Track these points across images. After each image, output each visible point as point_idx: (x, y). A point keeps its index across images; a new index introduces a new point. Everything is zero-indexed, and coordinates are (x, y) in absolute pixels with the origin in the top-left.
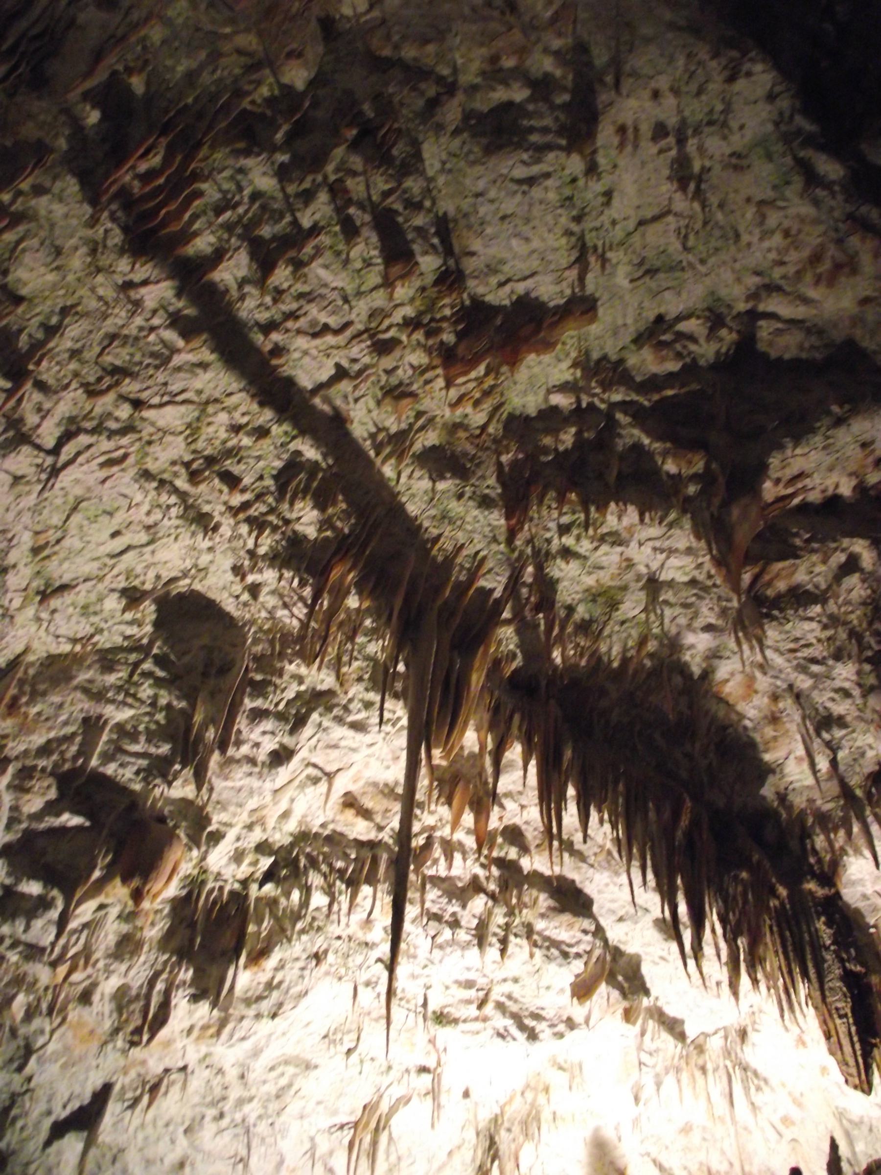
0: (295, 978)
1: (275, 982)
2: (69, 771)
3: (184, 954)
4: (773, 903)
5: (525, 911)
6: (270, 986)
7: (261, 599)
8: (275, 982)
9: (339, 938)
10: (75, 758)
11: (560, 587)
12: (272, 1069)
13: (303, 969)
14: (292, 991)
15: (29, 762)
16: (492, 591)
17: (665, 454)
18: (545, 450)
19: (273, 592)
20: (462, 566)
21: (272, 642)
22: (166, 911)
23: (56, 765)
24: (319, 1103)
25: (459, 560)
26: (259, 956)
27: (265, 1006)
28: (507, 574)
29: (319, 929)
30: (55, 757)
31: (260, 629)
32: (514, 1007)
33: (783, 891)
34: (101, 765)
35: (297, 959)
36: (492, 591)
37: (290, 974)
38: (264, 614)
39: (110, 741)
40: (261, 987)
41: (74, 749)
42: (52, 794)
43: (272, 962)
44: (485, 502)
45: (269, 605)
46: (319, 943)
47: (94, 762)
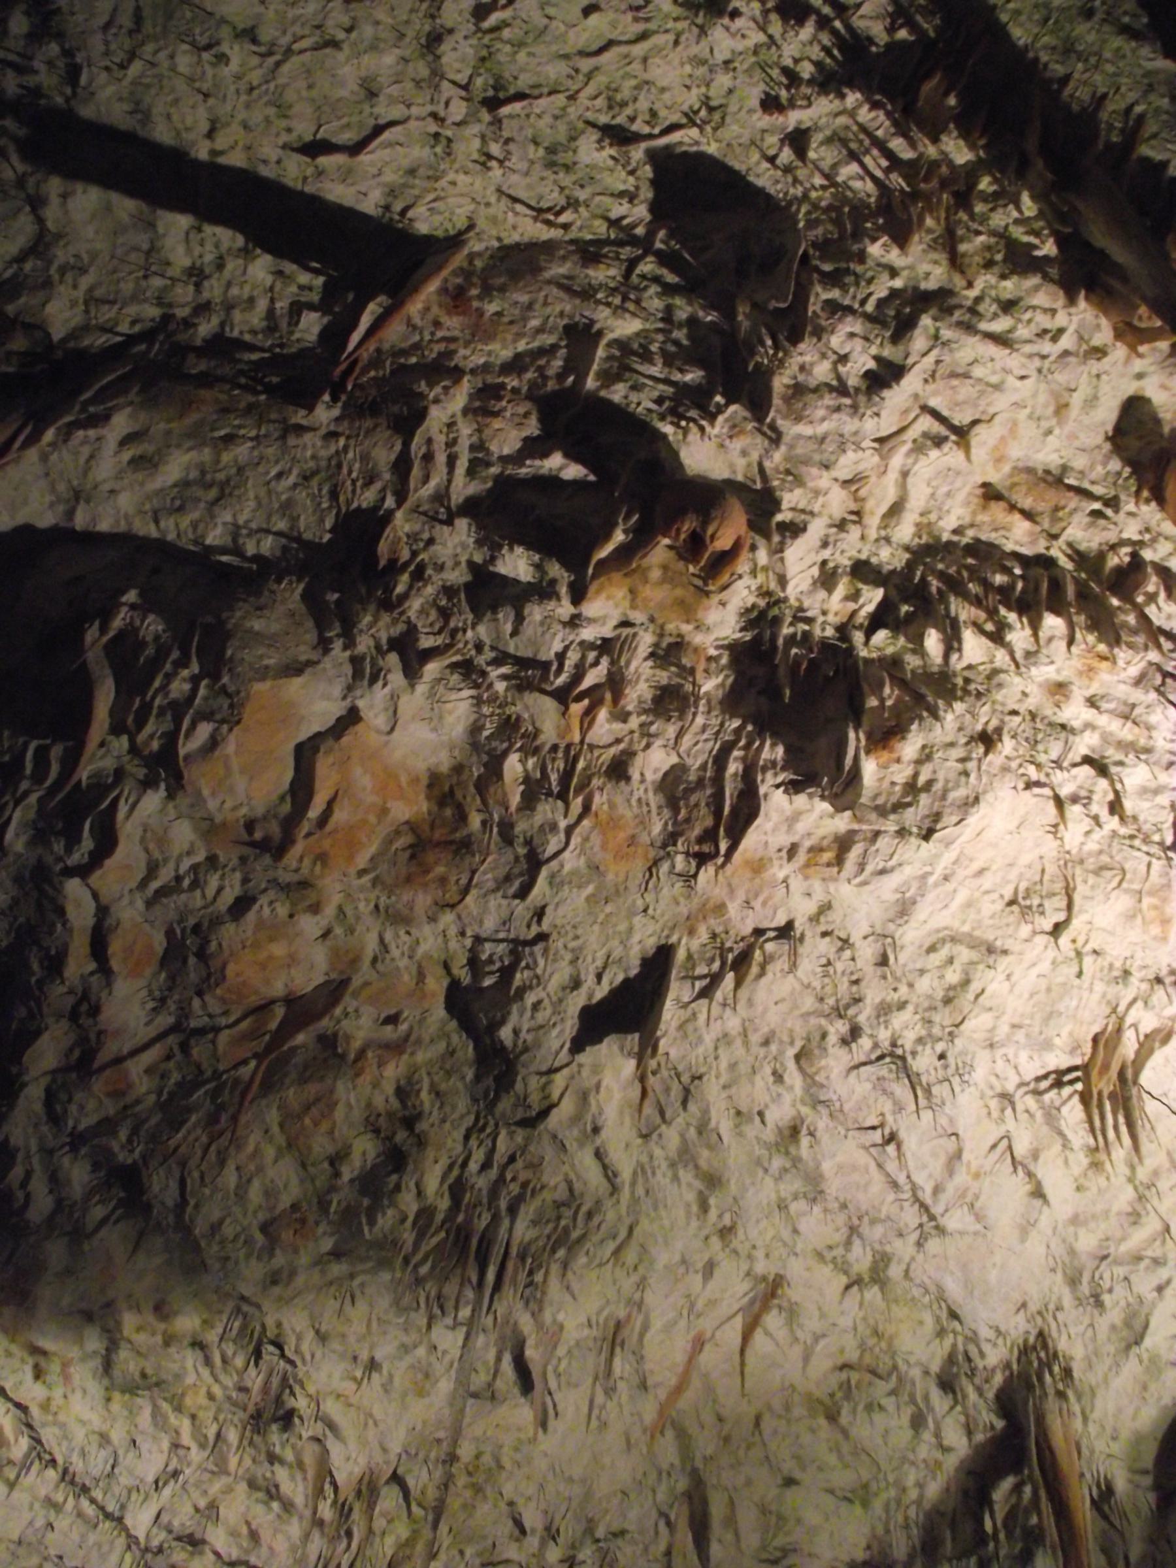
0: (952, 776)
1: (922, 780)
2: (555, 394)
3: (767, 723)
6: (912, 787)
7: (812, 155)
8: (922, 780)
9: (1014, 713)
10: (561, 377)
13: (963, 760)
15: (491, 379)
19: (829, 141)
21: (838, 222)
23: (533, 385)
26: (885, 736)
29: (979, 695)
30: (530, 375)
31: (815, 206)
34: (602, 387)
35: (952, 745)
37: (945, 767)
38: (818, 181)
39: (610, 358)
41: (558, 363)
42: (532, 428)
43: (910, 748)
45: (826, 165)
46: (985, 718)
47: (591, 383)
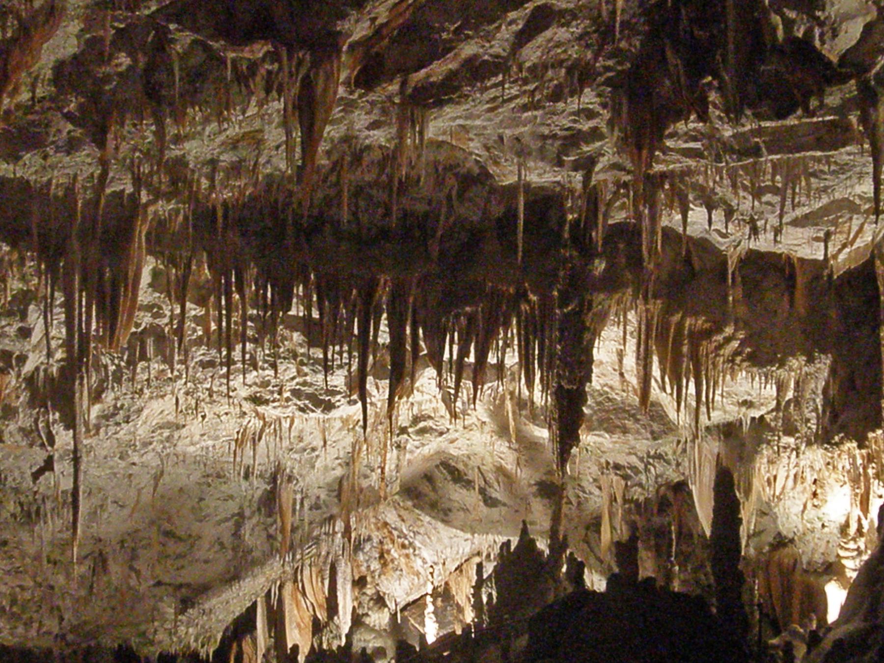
4: (524, 307)
5: (286, 343)
11: (191, 158)
12: (153, 432)
14: (132, 410)
16: (123, 191)
17: (225, 50)
18: (107, 79)
20: (85, 189)
22: (24, 386)
24: (202, 435)
25: (78, 185)
27: (119, 418)
28: (130, 176)
32: (309, 390)
33: (534, 298)
36: (123, 191)
40: (111, 408)
44: (72, 146)
